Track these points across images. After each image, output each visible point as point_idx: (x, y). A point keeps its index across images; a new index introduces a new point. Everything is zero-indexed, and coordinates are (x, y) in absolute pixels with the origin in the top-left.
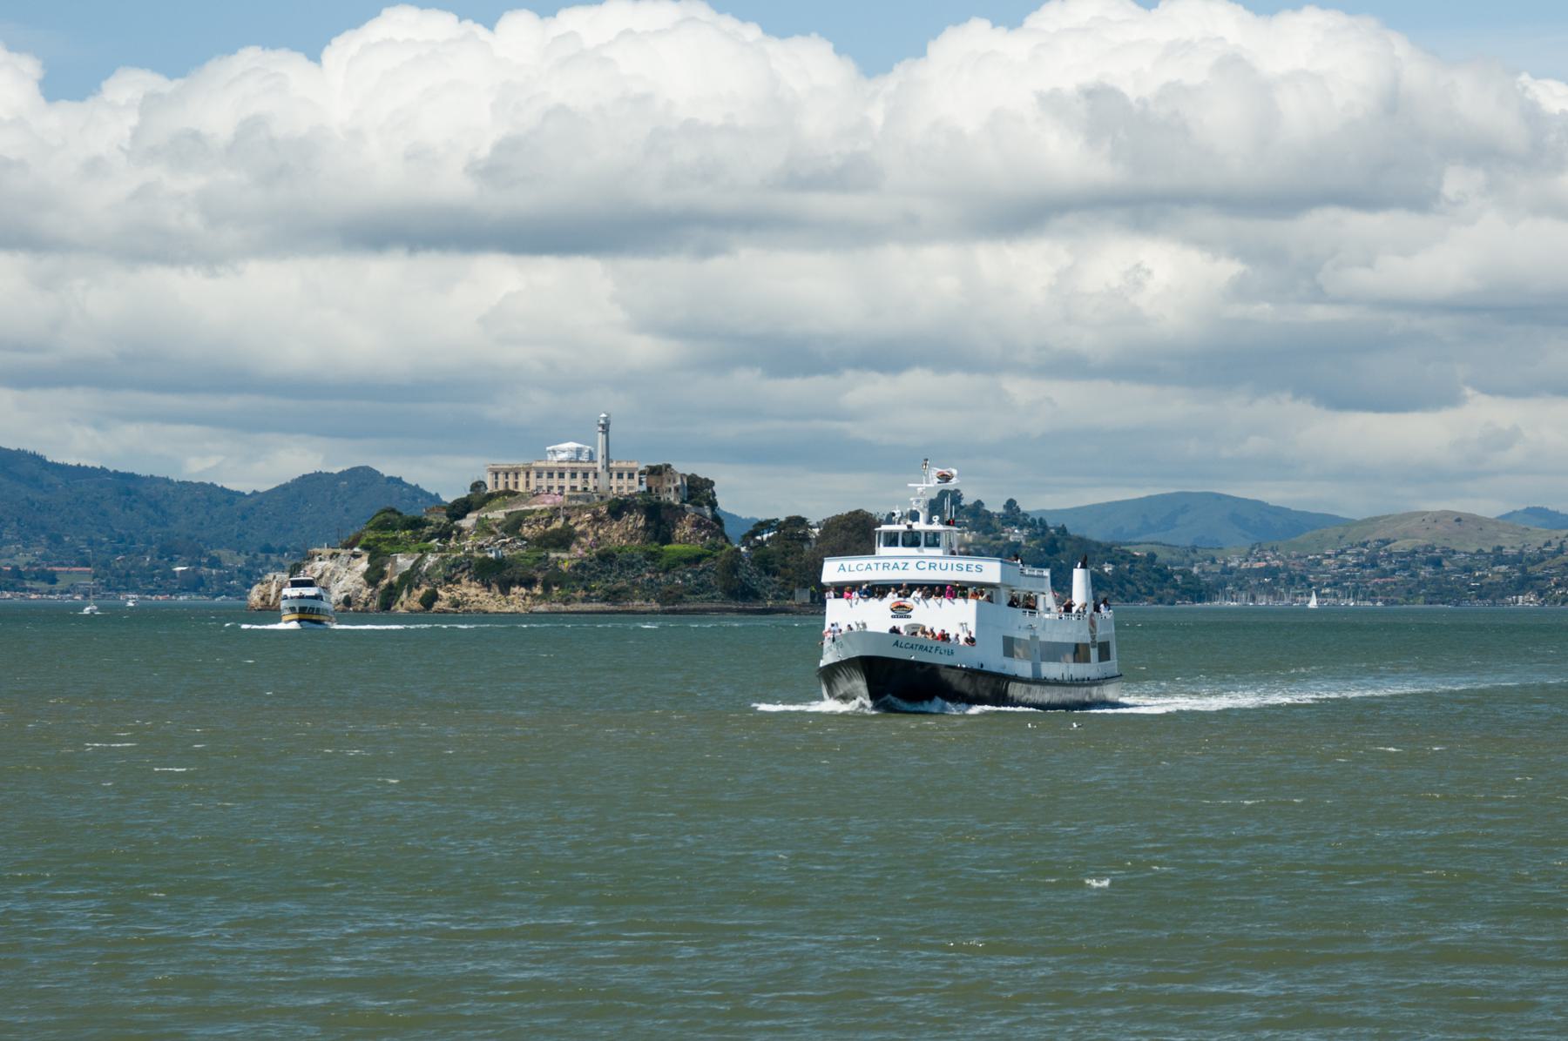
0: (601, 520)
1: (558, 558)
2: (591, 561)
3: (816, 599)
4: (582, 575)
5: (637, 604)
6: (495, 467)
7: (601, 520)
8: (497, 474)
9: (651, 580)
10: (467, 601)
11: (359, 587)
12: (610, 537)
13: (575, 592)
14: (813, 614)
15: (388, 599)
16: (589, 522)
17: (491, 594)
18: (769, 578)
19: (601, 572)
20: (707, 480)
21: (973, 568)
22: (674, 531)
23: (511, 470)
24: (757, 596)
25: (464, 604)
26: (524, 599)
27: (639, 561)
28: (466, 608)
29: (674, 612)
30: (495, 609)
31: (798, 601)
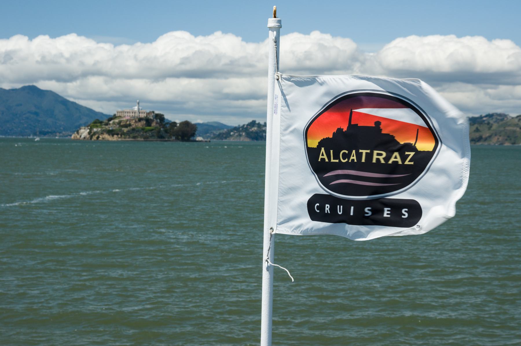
4: (128, 133)
5: (139, 139)
15: (91, 137)
29: (146, 141)
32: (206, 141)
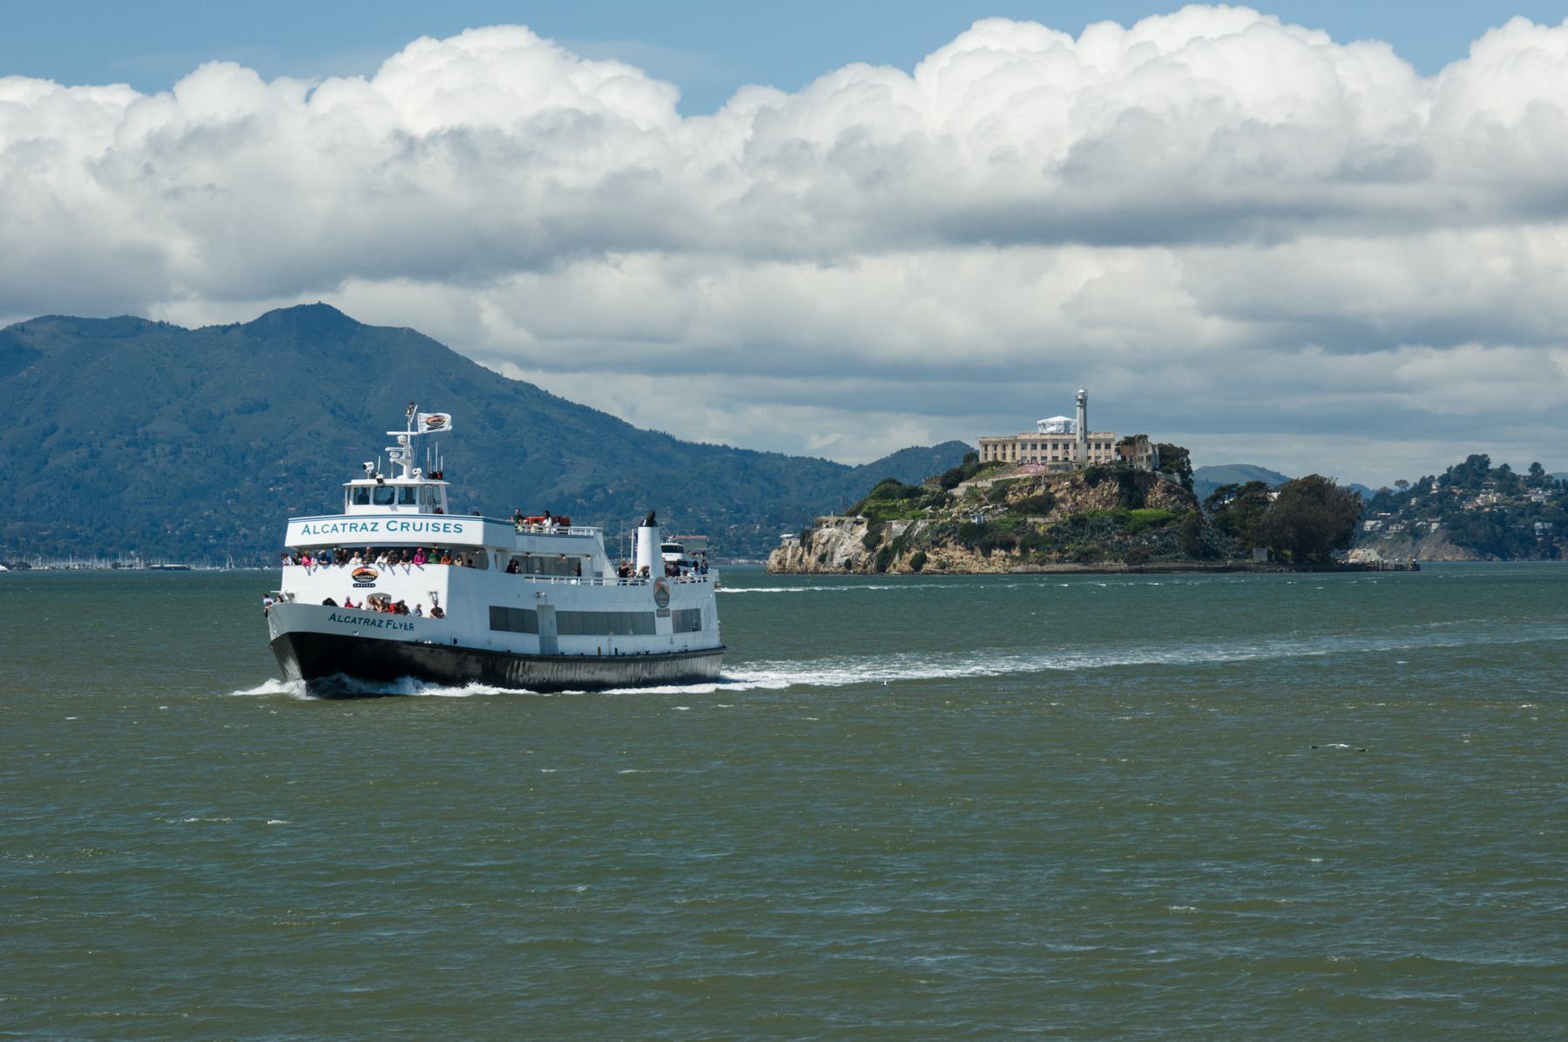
0: (1079, 487)
1: (1035, 523)
2: (1065, 525)
3: (1273, 558)
4: (1057, 538)
6: (984, 440)
7: (1079, 487)
8: (986, 447)
9: (1120, 542)
10: (953, 562)
11: (859, 550)
13: (1050, 554)
14: (1269, 571)
15: (884, 560)
16: (1068, 489)
17: (974, 557)
19: (1073, 535)
20: (1182, 449)
21: (452, 528)
22: (1147, 496)
23: (1000, 442)
24: (1218, 555)
25: (949, 566)
26: (1004, 560)
27: (1109, 525)
28: (952, 569)
29: (1141, 571)
30: (977, 570)
32: (1399, 568)
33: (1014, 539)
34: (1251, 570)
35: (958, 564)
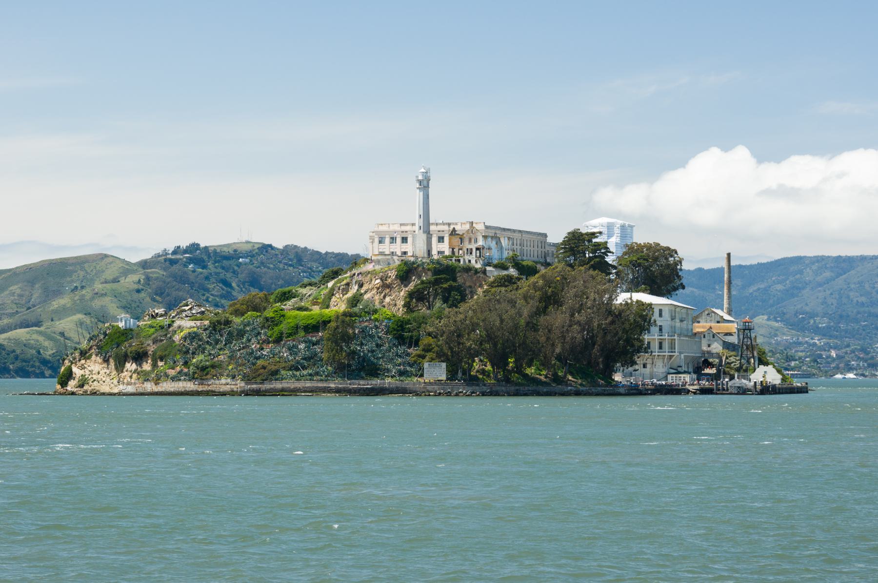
0: (389, 286)
5: (223, 383)
7: (389, 286)
12: (395, 305)
16: (378, 289)
17: (108, 372)
18: (401, 349)
20: (668, 249)
24: (374, 371)
29: (258, 393)
31: (428, 377)
33: (148, 348)
34: (417, 394)
35: (95, 380)
